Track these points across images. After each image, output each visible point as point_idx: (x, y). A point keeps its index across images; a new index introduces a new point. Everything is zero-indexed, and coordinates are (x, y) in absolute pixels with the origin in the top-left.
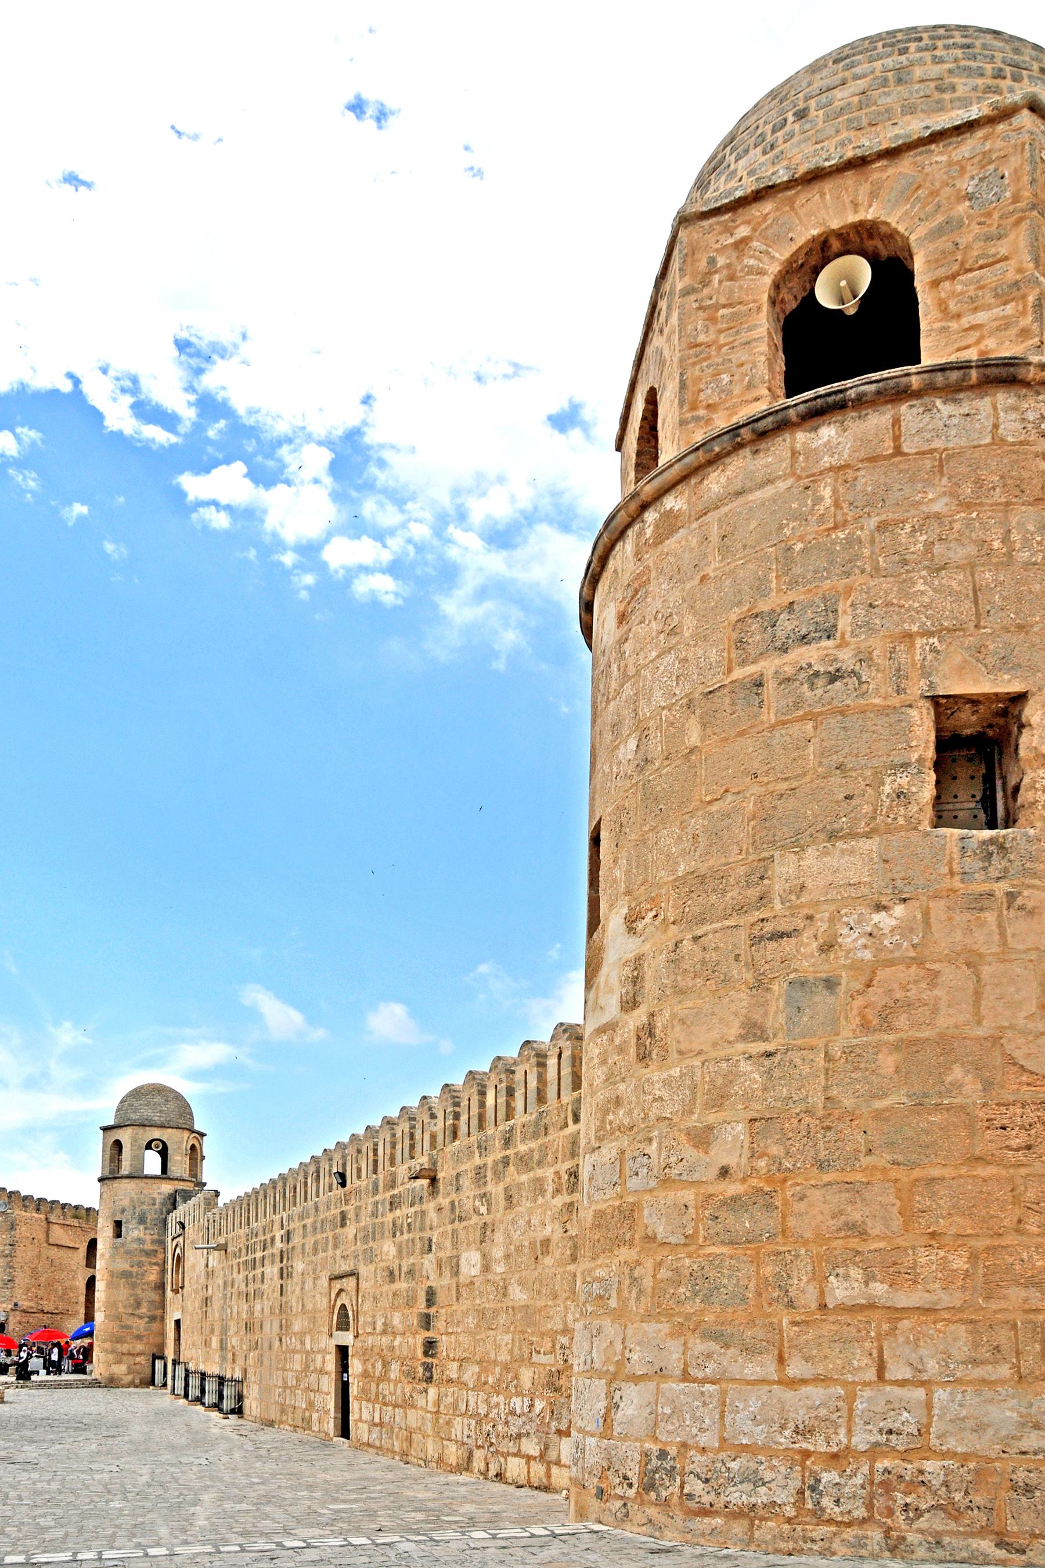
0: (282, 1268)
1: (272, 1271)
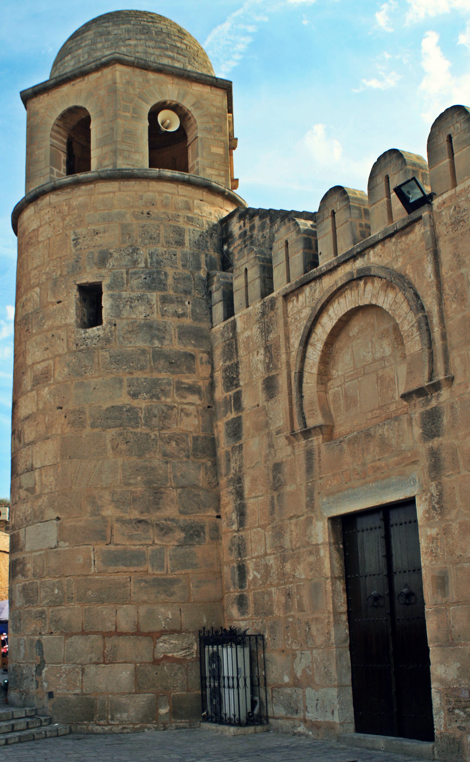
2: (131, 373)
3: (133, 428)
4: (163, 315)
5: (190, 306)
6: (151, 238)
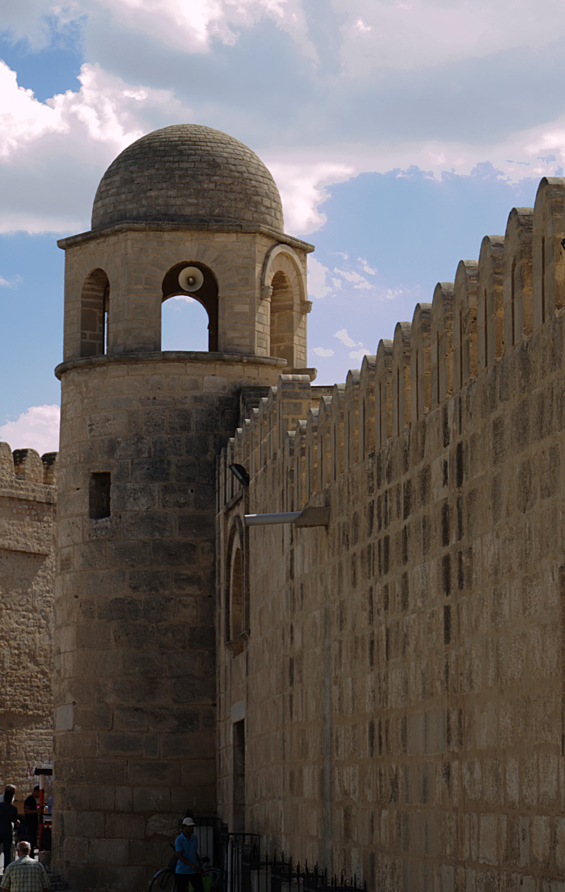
0: (446, 560)
1: (424, 571)
2: (133, 566)
3: (133, 620)
4: (164, 506)
5: (192, 495)
6: (155, 425)
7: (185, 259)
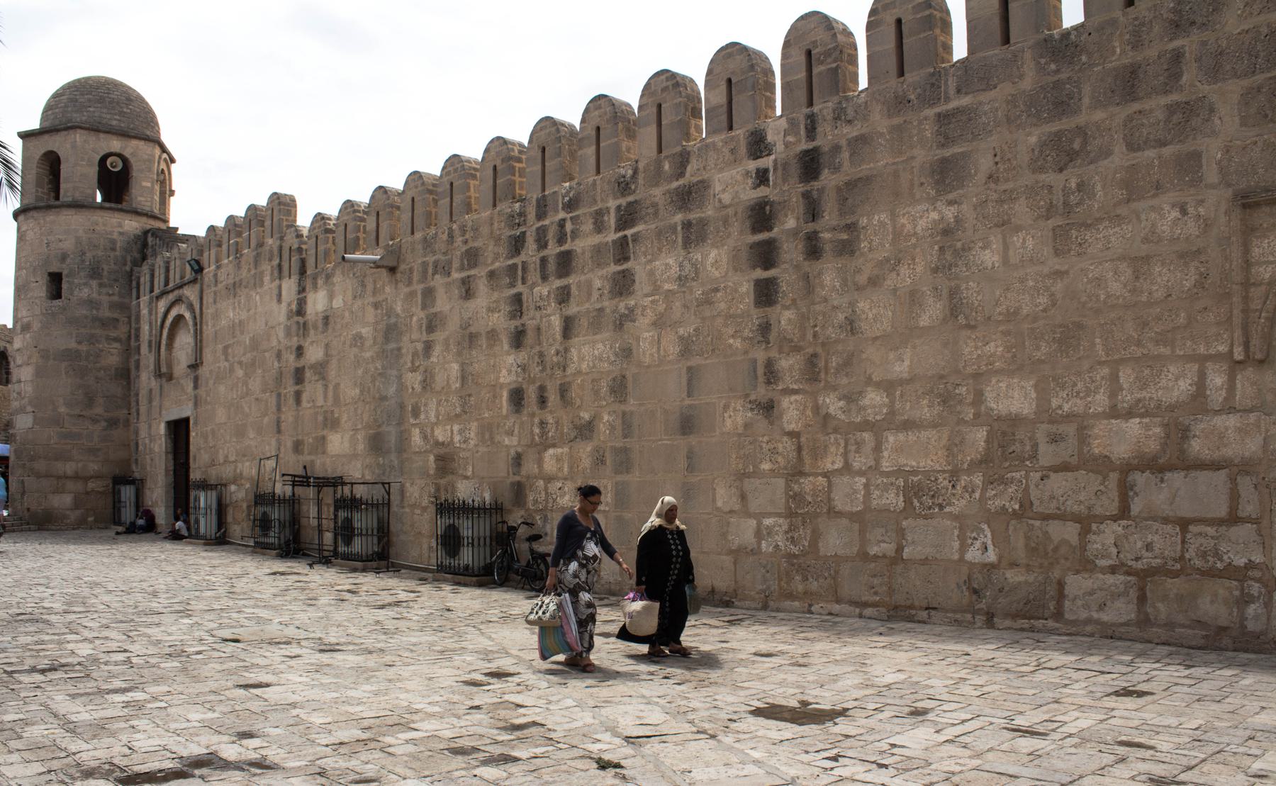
7: (107, 151)
